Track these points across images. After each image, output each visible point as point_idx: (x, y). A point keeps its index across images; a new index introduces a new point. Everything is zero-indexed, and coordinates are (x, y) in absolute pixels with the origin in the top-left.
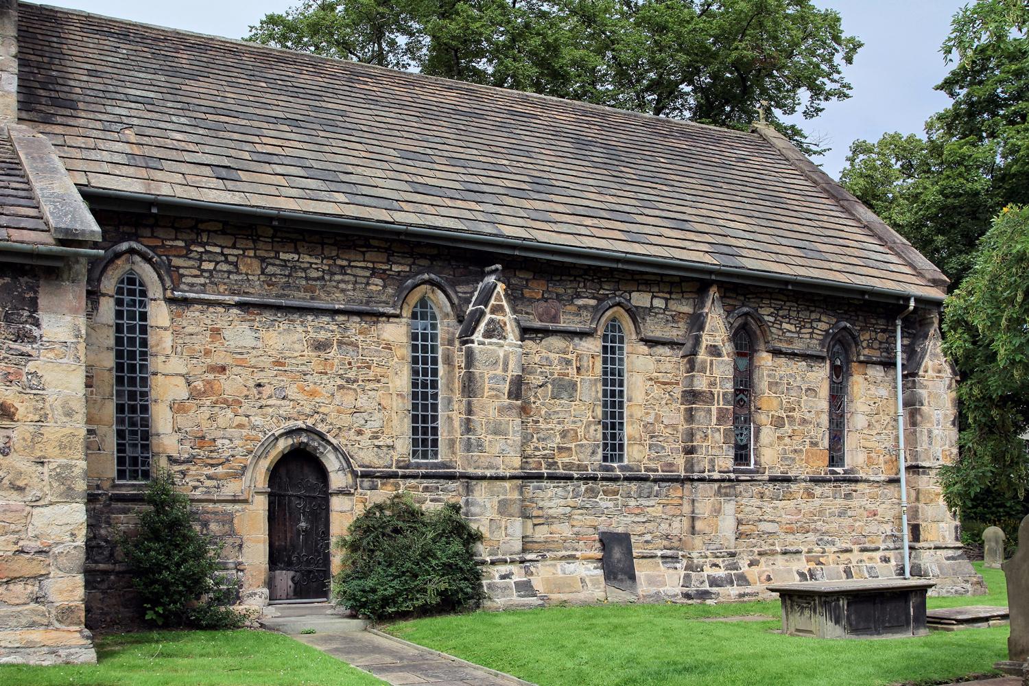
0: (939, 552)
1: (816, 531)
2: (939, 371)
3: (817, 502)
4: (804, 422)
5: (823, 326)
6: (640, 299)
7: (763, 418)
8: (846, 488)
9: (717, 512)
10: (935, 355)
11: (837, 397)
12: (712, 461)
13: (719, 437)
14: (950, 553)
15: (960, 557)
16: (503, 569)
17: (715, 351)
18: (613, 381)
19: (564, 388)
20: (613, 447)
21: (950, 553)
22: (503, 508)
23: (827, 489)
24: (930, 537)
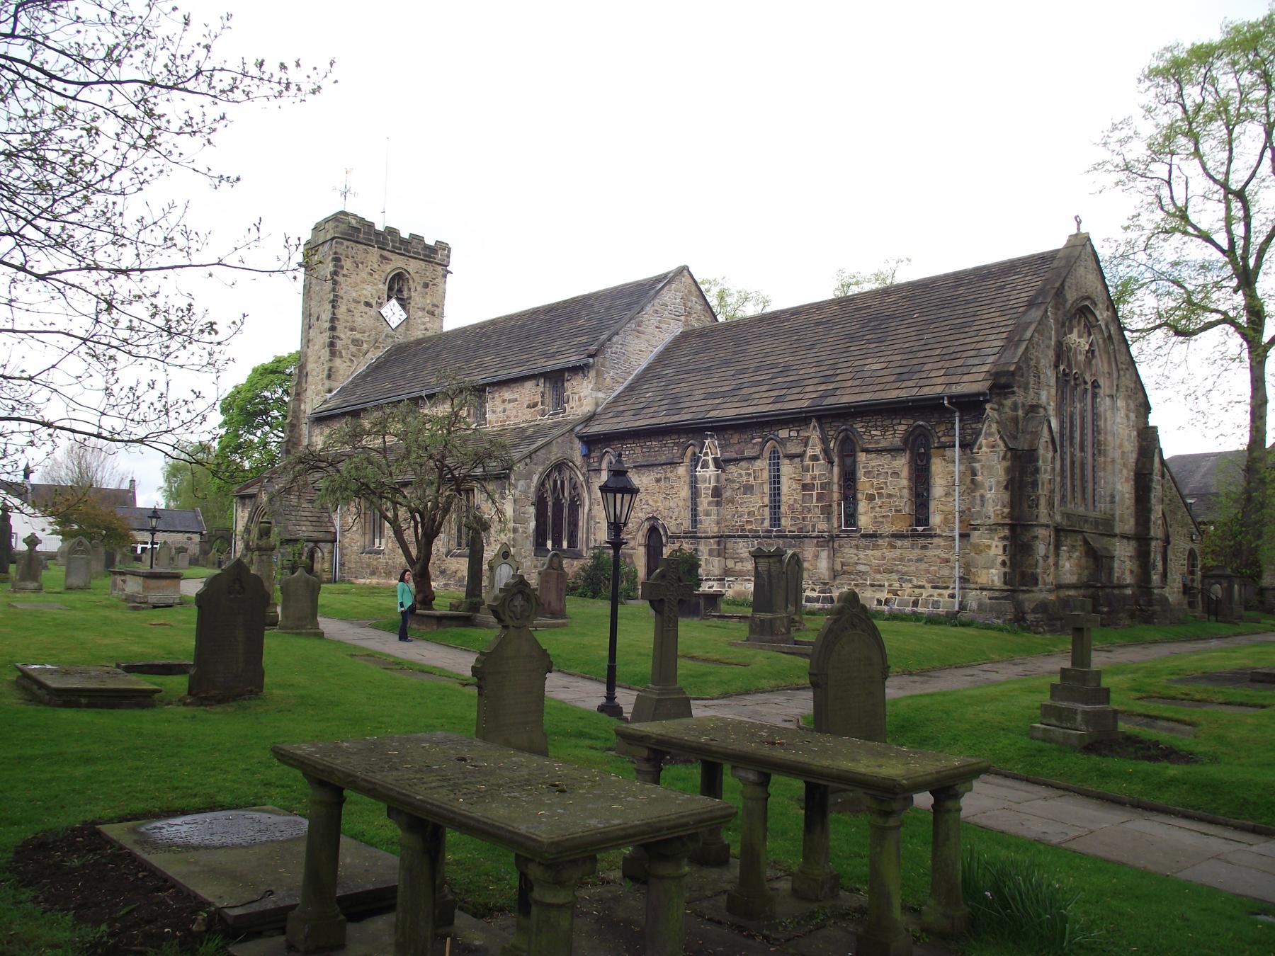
1: (897, 572)
3: (898, 551)
4: (890, 496)
5: (903, 427)
6: (783, 433)
7: (859, 496)
8: (922, 542)
9: (817, 557)
10: (989, 434)
12: (814, 526)
13: (818, 511)
15: (1004, 598)
16: (711, 583)
17: (815, 458)
18: (775, 480)
19: (748, 489)
20: (776, 520)
21: (997, 594)
22: (711, 553)
23: (907, 543)
24: (979, 580)
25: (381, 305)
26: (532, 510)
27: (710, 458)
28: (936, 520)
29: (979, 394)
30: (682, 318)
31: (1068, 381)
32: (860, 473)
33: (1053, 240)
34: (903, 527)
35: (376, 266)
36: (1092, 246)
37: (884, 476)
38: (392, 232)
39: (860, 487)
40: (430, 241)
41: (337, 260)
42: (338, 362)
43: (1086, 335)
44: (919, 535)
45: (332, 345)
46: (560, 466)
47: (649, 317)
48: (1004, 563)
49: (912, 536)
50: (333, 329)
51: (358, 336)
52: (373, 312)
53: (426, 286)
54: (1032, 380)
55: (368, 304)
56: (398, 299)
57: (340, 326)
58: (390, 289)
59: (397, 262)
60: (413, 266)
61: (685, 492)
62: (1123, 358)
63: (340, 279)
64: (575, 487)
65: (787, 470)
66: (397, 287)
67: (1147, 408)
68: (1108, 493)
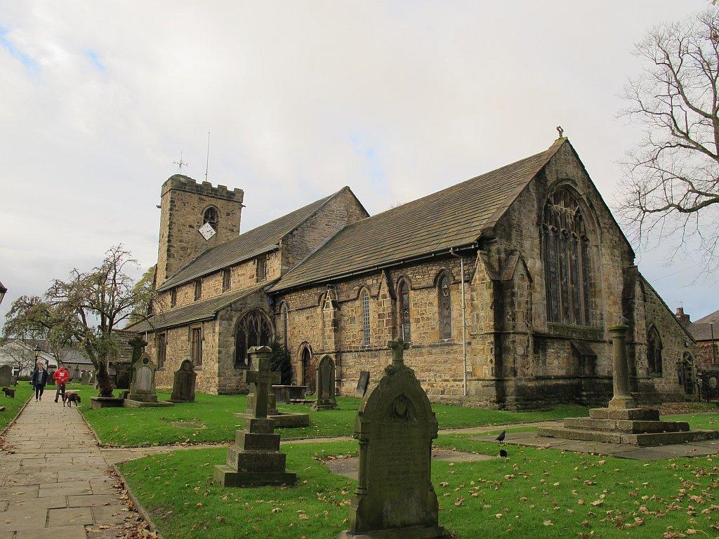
0: (481, 382)
1: (433, 371)
2: (483, 280)
3: (433, 357)
4: (428, 319)
5: (434, 272)
6: (369, 282)
8: (446, 349)
10: (481, 271)
11: (445, 304)
13: (387, 331)
14: (487, 383)
15: (491, 386)
17: (384, 297)
18: (366, 313)
21: (487, 383)
25: (199, 227)
26: (232, 339)
27: (330, 301)
28: (454, 333)
29: (470, 245)
30: (346, 219)
31: (557, 236)
32: (411, 305)
33: (542, 143)
34: (434, 339)
35: (196, 205)
36: (571, 146)
37: (423, 303)
38: (207, 185)
39: (411, 314)
40: (231, 189)
41: (172, 202)
42: (172, 260)
43: (573, 206)
44: (445, 345)
45: (168, 250)
46: (254, 312)
47: (322, 222)
48: (491, 361)
49: (441, 345)
50: (169, 241)
51: (185, 245)
52: (194, 231)
53: (228, 214)
54: (514, 233)
55: (191, 226)
56: (210, 223)
57: (173, 240)
58: (206, 217)
59: (209, 202)
60: (219, 204)
61: (320, 326)
62: (606, 221)
63: (174, 212)
64: (265, 325)
65: (372, 305)
66: (210, 216)
67: (631, 254)
68: (598, 312)
